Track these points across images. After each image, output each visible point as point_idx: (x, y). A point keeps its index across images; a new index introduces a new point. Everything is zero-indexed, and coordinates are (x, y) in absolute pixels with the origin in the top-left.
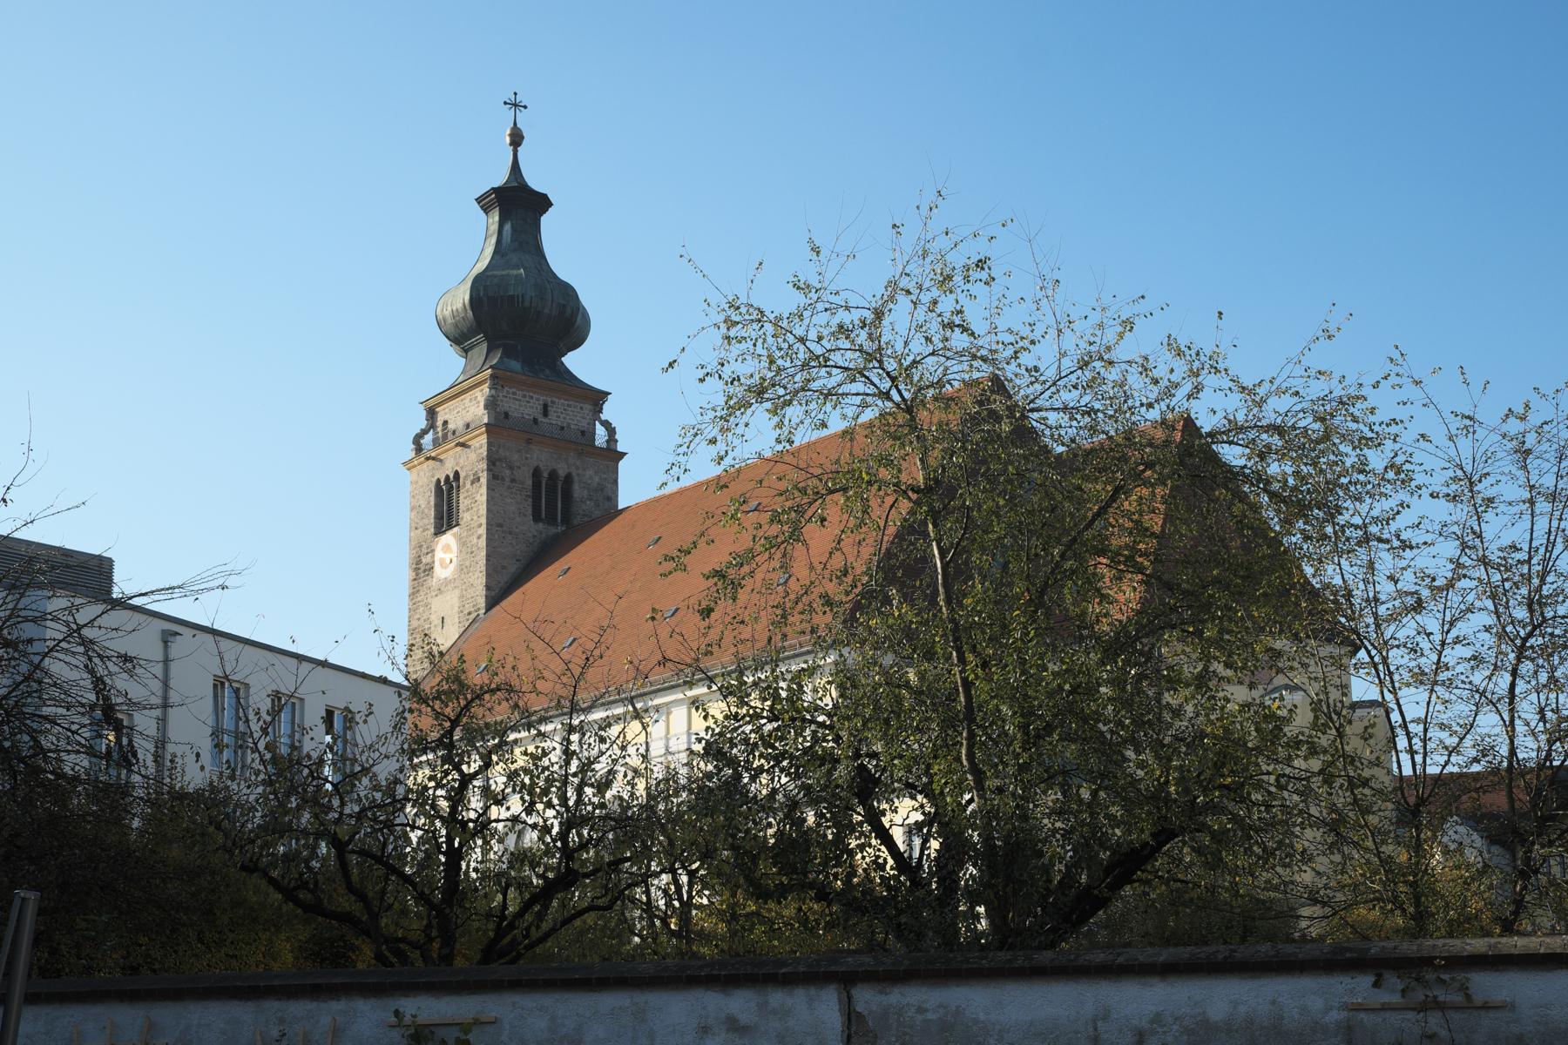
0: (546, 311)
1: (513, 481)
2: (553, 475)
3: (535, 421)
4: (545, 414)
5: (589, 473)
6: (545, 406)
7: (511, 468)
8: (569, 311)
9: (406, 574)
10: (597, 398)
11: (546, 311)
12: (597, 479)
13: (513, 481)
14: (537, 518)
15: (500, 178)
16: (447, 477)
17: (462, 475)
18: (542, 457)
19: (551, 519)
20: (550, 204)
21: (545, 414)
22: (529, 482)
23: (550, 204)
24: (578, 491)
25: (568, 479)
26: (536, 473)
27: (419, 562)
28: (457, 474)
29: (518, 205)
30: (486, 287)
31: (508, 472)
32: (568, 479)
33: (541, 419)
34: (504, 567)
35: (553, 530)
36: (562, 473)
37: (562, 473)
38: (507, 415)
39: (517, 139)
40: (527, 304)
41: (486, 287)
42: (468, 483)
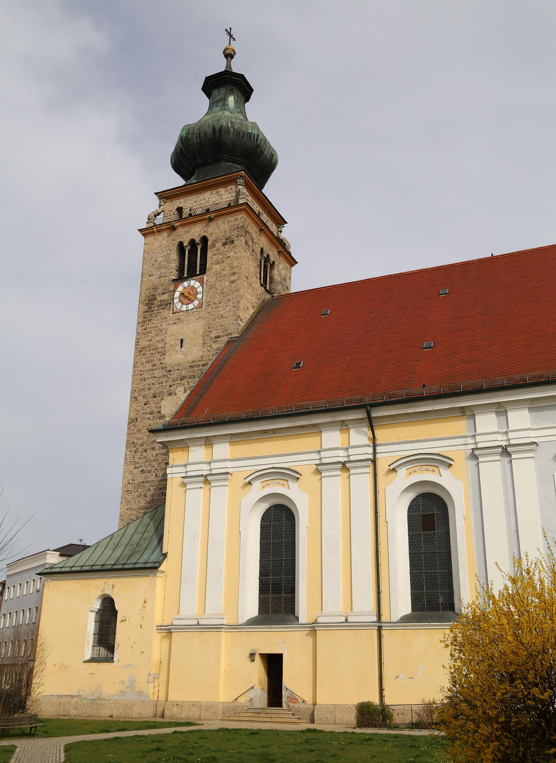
0: (266, 153)
16: (192, 242)
28: (205, 240)
30: (232, 122)
40: (259, 142)
42: (219, 245)
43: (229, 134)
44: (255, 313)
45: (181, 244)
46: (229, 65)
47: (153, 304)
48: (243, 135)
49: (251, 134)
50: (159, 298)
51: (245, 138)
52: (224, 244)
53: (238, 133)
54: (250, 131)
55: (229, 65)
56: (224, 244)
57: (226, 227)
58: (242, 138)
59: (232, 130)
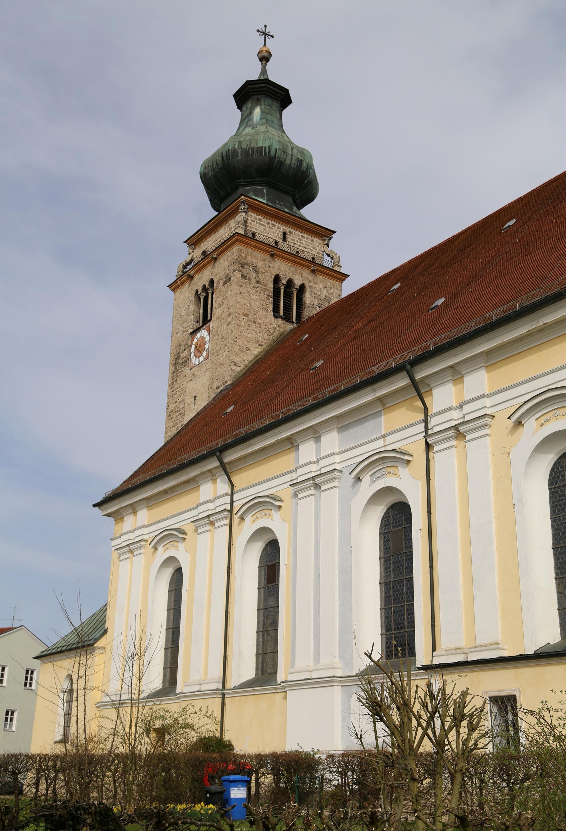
0: (287, 162)
1: (258, 282)
5: (319, 286)
6: (285, 234)
7: (257, 272)
8: (304, 165)
10: (325, 234)
12: (325, 292)
13: (258, 282)
17: (216, 281)
19: (287, 318)
22: (271, 286)
24: (308, 298)
26: (277, 279)
28: (212, 282)
30: (240, 142)
31: (254, 275)
32: (302, 288)
34: (248, 349)
35: (289, 327)
36: (298, 283)
37: (298, 283)
40: (272, 154)
41: (240, 142)
43: (237, 156)
44: (262, 352)
48: (253, 152)
49: (261, 148)
51: (255, 155)
52: (225, 283)
53: (246, 152)
56: (225, 283)
58: (252, 156)
59: (239, 151)
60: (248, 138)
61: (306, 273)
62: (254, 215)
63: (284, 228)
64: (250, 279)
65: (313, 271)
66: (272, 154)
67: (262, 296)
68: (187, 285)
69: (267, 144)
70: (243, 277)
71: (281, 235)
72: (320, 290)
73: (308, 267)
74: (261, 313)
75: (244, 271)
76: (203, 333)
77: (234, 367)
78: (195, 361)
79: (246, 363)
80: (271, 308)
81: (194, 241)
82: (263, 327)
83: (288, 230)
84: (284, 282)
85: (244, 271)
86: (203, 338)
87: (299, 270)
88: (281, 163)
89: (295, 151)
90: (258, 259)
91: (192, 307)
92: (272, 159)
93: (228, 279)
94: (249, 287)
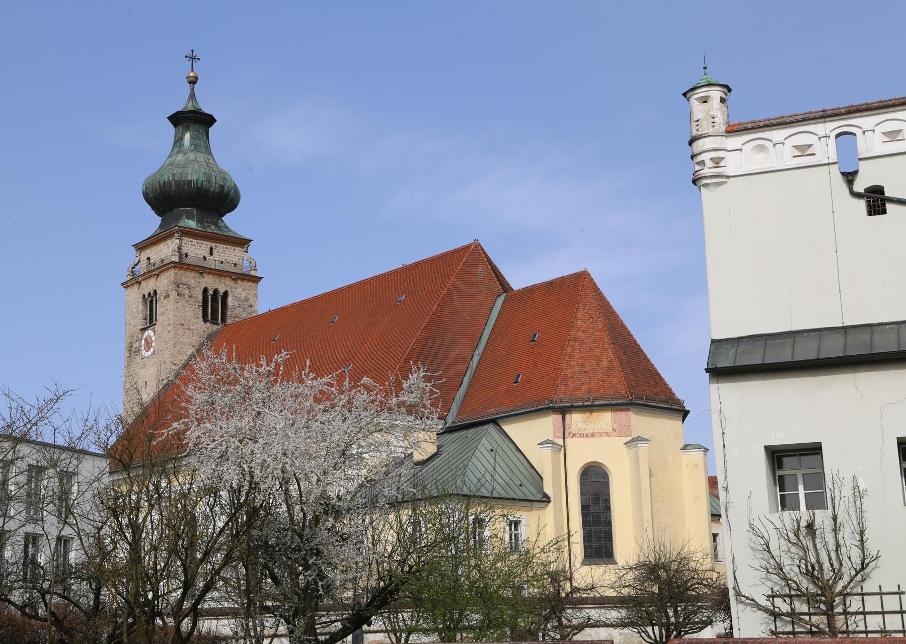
0: (212, 189)
1: (190, 297)
2: (216, 291)
3: (205, 258)
4: (211, 254)
5: (239, 290)
6: (211, 249)
7: (189, 289)
9: (124, 354)
10: (243, 243)
11: (212, 189)
12: (244, 294)
13: (190, 297)
14: (205, 320)
15: (180, 104)
16: (150, 294)
17: (158, 292)
18: (211, 282)
19: (214, 321)
20: (215, 121)
21: (211, 254)
22: (201, 297)
23: (215, 121)
24: (230, 300)
25: (226, 294)
26: (205, 291)
27: (131, 346)
28: (155, 292)
29: (193, 121)
30: (173, 175)
31: (187, 291)
32: (226, 294)
33: (208, 257)
35: (215, 327)
36: (222, 291)
37: (222, 291)
38: (186, 255)
39: (193, 82)
40: (199, 185)
41: (173, 175)
42: (162, 298)
45: (144, 296)
46: (192, 96)
47: (132, 351)
50: (135, 346)
51: (186, 187)
52: (165, 298)
53: (178, 183)
54: (189, 178)
55: (192, 96)
56: (165, 298)
57: (165, 281)
60: (180, 171)
61: (228, 281)
62: (186, 239)
63: (210, 244)
64: (184, 296)
65: (234, 279)
66: (199, 185)
67: (194, 307)
68: (136, 287)
69: (195, 177)
70: (179, 295)
71: (208, 250)
72: (240, 293)
73: (230, 277)
74: (194, 321)
75: (179, 290)
76: (149, 332)
77: (173, 367)
78: (144, 353)
79: (183, 362)
80: (201, 315)
81: (141, 247)
82: (195, 331)
83: (213, 245)
84: (211, 292)
85: (179, 290)
86: (150, 337)
87: (223, 280)
88: (207, 191)
89: (218, 178)
90: (190, 278)
91: (141, 308)
92: (199, 189)
93: (167, 296)
94: (183, 302)
